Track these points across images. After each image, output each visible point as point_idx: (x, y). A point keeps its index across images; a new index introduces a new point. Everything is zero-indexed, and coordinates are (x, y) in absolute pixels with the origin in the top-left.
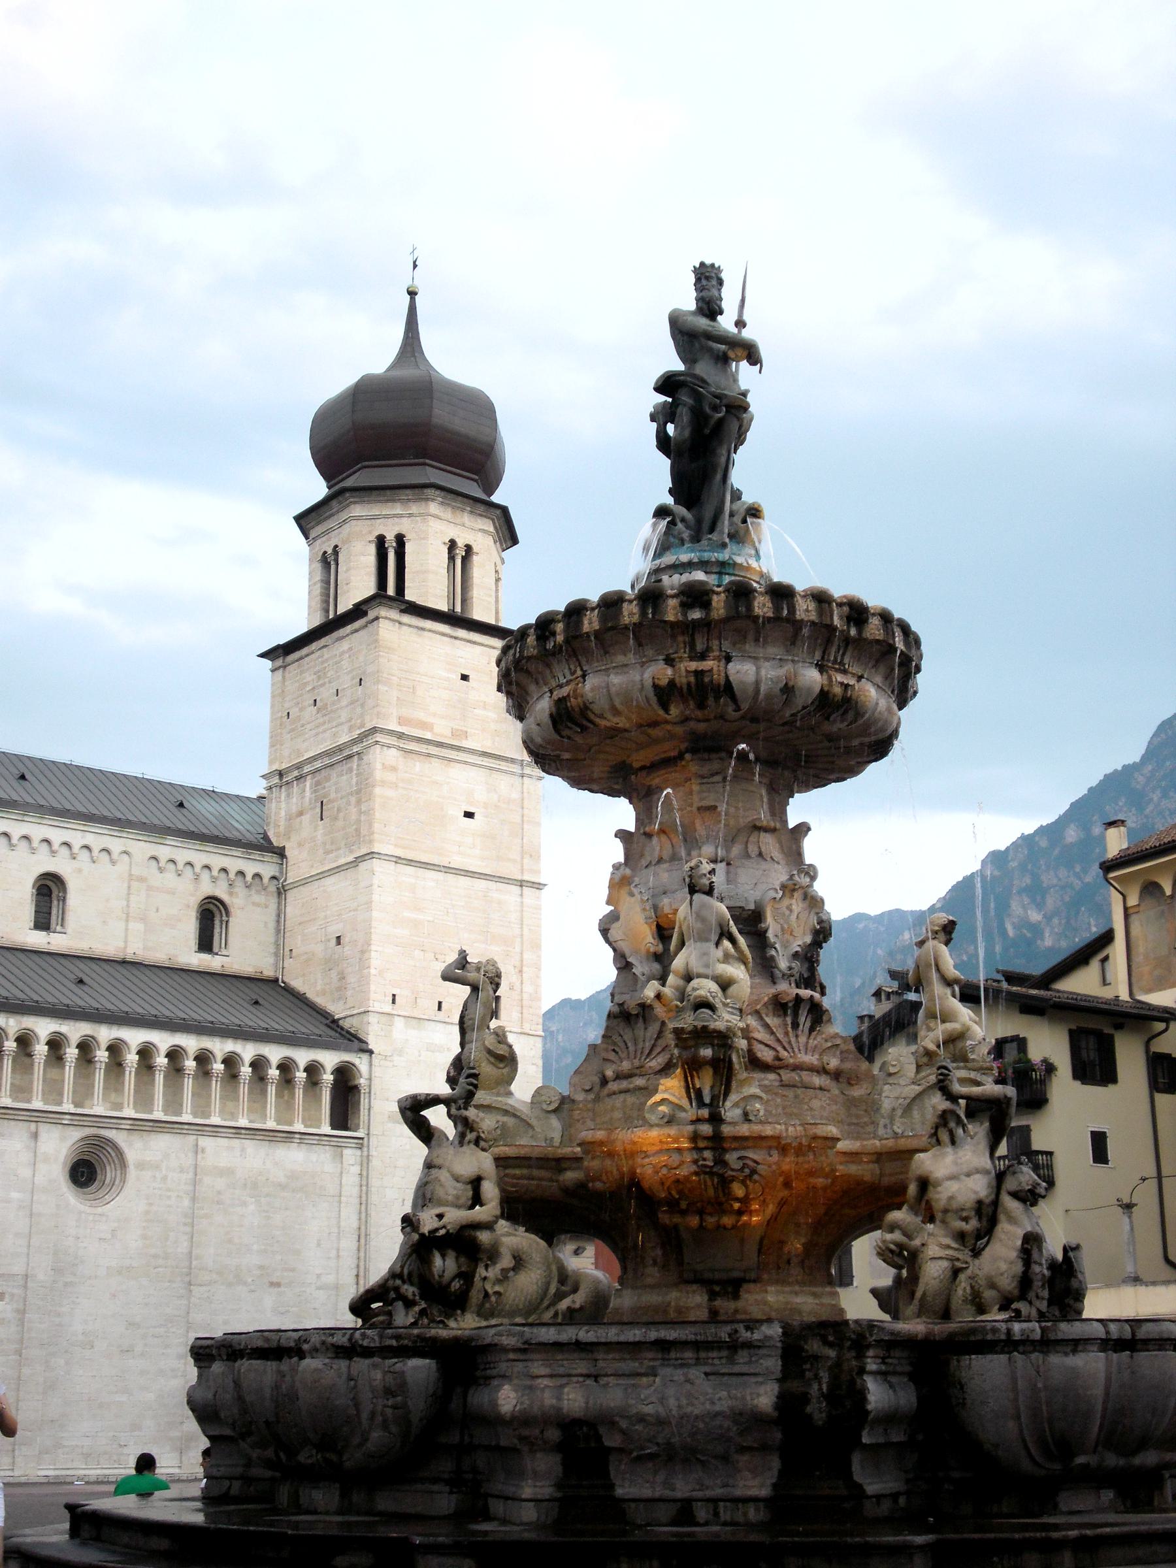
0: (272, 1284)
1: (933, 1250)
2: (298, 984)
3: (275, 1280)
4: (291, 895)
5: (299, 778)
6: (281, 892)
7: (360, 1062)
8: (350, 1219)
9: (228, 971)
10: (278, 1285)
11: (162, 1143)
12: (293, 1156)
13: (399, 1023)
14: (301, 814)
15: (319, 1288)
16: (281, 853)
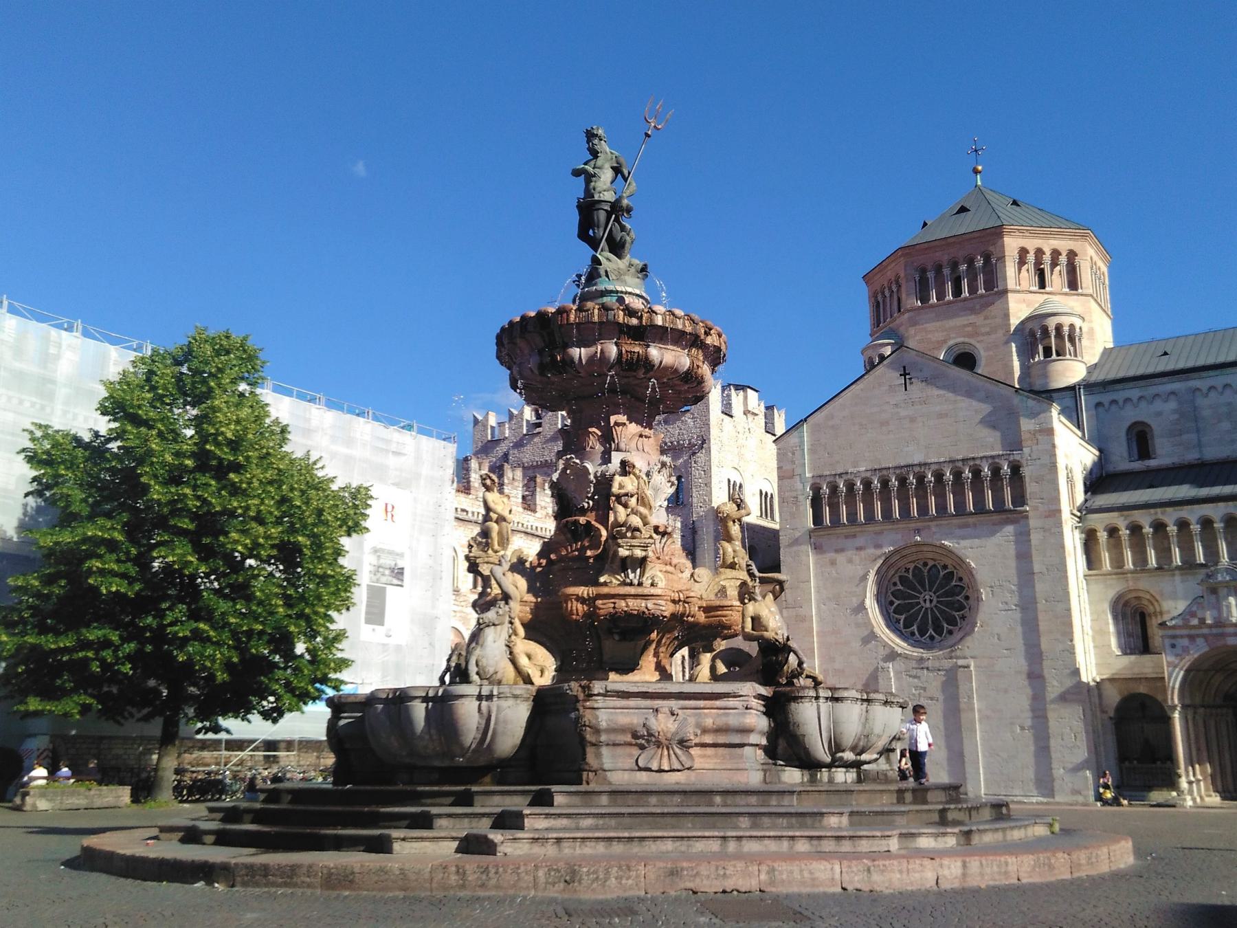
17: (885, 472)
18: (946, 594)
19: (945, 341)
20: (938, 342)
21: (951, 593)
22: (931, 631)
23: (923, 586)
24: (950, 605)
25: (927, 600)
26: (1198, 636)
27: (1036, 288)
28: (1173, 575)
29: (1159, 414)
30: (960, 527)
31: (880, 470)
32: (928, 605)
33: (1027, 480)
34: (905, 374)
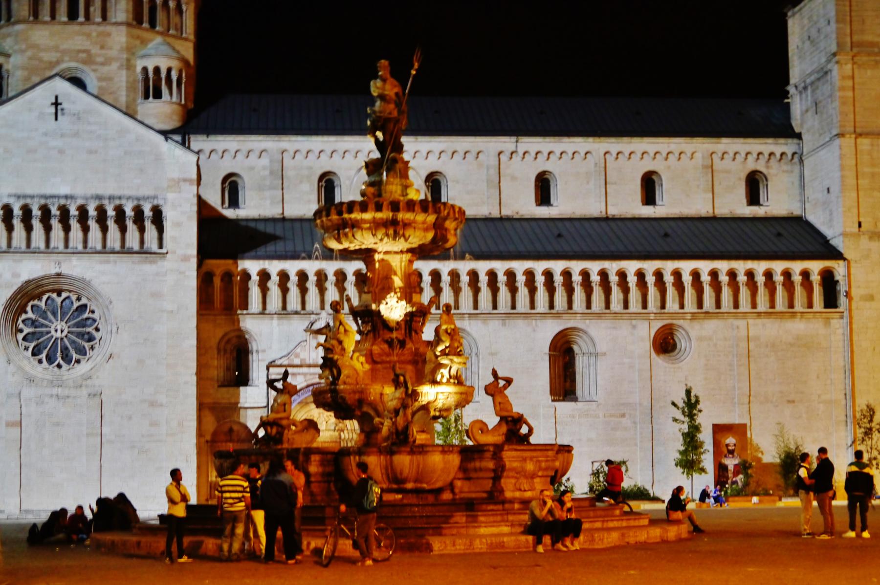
0: (789, 402)
1: (386, 424)
2: (812, 218)
3: (791, 398)
4: (805, 162)
5: (805, 88)
6: (801, 161)
7: (839, 269)
8: (839, 360)
9: (770, 214)
10: (793, 402)
11: (710, 326)
12: (797, 327)
13: (864, 241)
14: (807, 111)
15: (819, 403)
16: (799, 136)
17: (28, 201)
18: (77, 325)
19: (58, 63)
20: (51, 63)
21: (83, 324)
22: (59, 360)
23: (54, 314)
24: (81, 335)
25: (58, 329)
26: (299, 374)
27: (146, 25)
28: (272, 319)
29: (252, 168)
30: (101, 262)
31: (25, 197)
32: (59, 334)
33: (167, 225)
34: (56, 104)
